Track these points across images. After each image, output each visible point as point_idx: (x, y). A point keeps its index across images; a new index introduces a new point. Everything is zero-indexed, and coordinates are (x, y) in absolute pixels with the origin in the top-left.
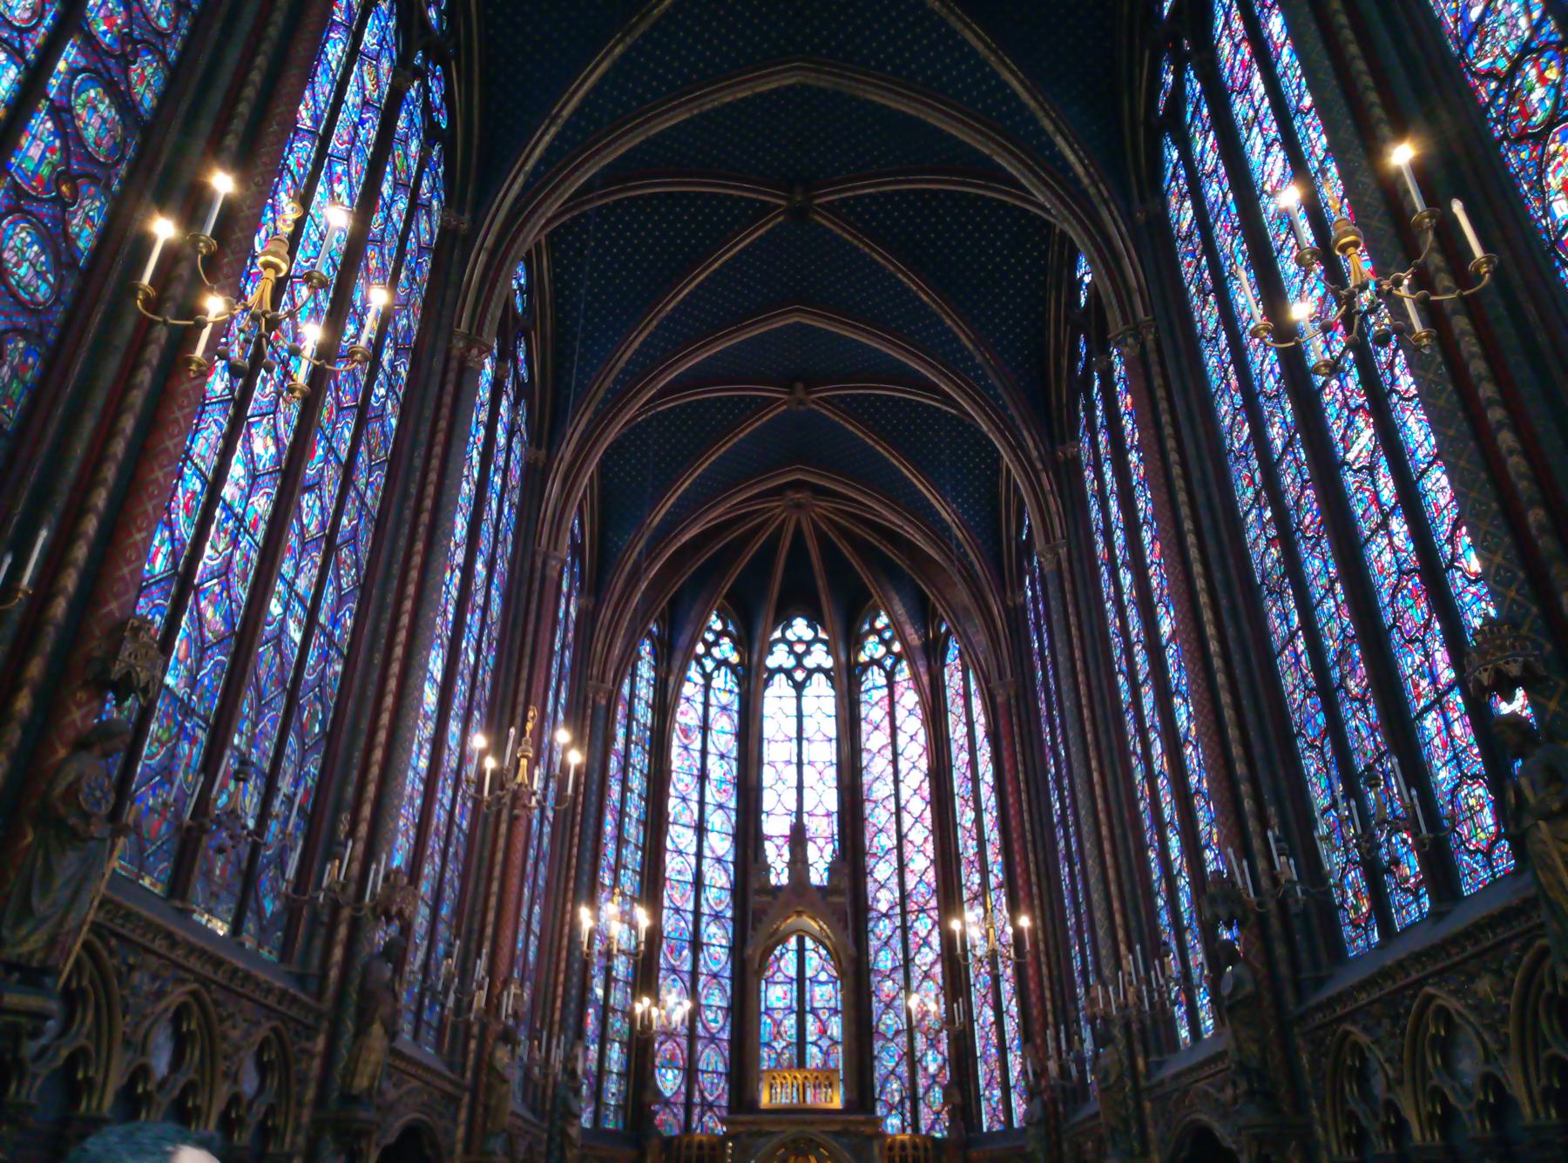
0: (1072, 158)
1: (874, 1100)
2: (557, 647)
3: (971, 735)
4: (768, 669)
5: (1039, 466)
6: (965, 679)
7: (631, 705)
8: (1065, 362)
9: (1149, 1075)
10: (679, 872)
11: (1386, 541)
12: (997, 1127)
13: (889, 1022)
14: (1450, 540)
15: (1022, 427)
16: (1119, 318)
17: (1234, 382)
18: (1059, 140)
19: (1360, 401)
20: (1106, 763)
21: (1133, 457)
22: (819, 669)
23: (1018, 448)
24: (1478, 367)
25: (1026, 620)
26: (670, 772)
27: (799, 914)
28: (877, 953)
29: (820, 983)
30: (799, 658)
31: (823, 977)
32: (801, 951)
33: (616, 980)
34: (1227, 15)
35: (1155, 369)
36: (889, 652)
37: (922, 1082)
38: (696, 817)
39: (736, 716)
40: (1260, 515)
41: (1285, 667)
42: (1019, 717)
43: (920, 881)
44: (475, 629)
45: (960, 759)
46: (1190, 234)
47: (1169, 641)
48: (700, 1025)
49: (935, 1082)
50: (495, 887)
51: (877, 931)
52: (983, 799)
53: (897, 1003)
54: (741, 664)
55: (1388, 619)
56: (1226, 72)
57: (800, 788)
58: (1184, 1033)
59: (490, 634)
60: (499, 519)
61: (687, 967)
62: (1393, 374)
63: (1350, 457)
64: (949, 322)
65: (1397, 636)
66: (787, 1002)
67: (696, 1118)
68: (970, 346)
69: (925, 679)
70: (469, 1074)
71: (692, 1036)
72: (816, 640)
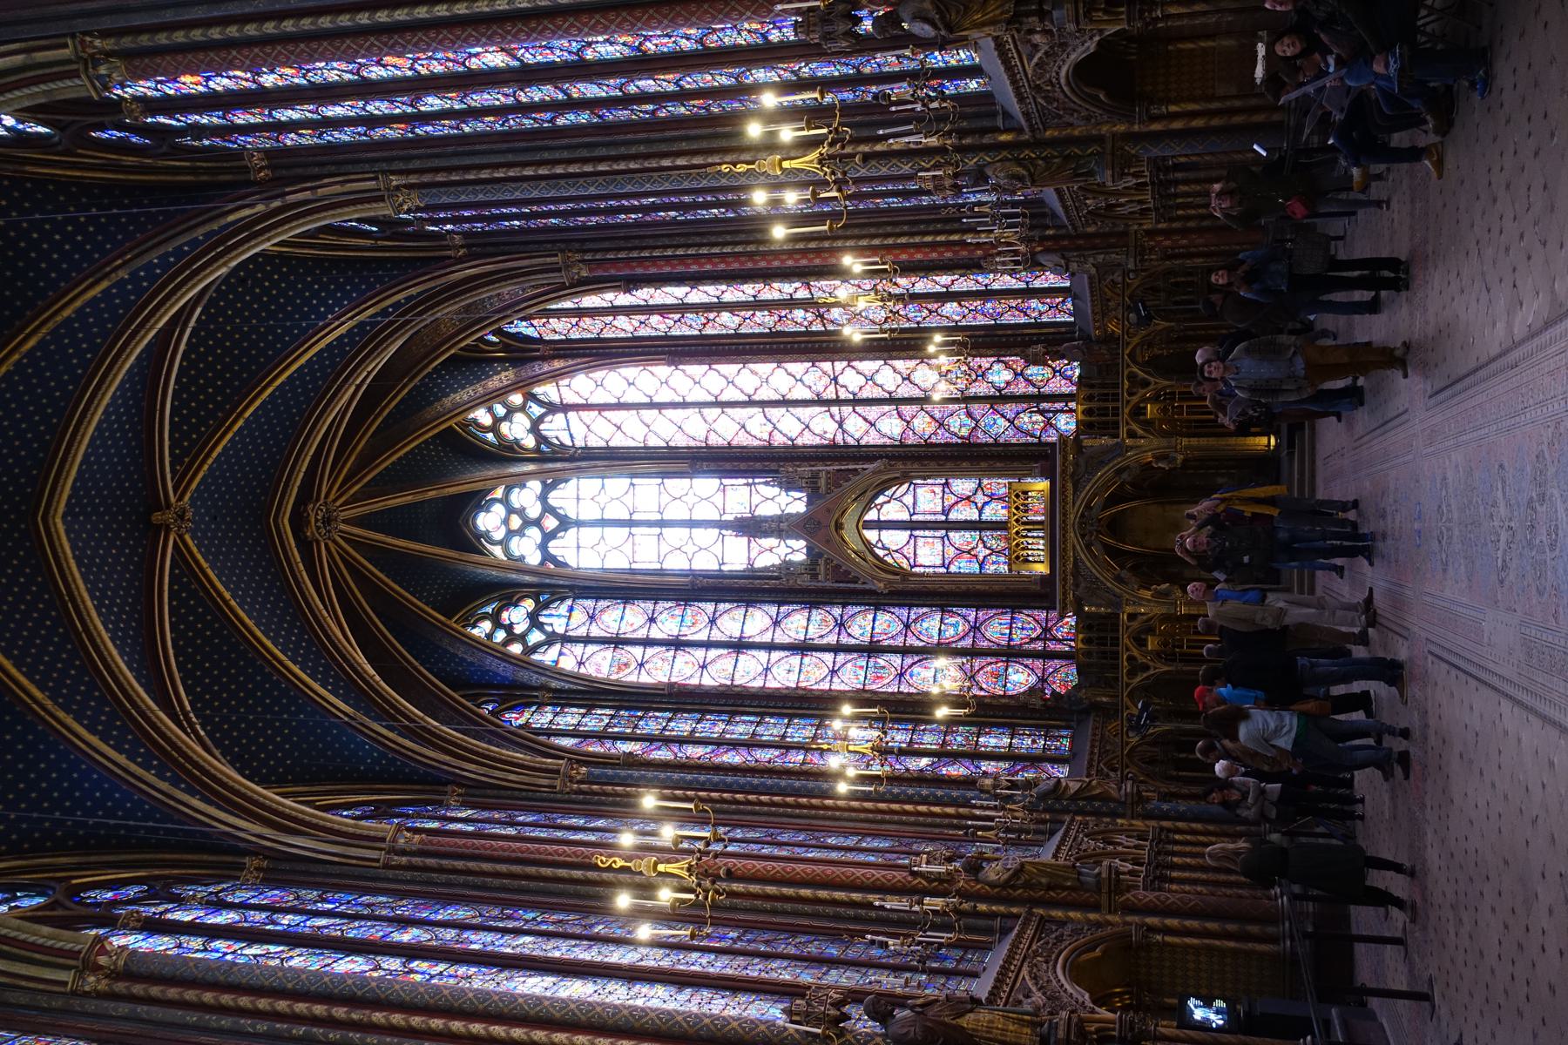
1: (1040, 444)
2: (511, 831)
3: (629, 311)
4: (542, 563)
5: (276, 204)
6: (559, 314)
7: (586, 736)
8: (130, 160)
9: (1020, 130)
12: (1069, 305)
13: (959, 424)
15: (223, 222)
16: (69, 83)
20: (664, 148)
21: (268, 80)
22: (543, 498)
23: (251, 228)
25: (484, 233)
26: (671, 685)
27: (839, 526)
30: (527, 523)
31: (908, 499)
32: (881, 525)
35: (144, 40)
36: (522, 409)
37: (1021, 388)
38: (725, 651)
39: (602, 604)
42: (608, 250)
44: (489, 937)
45: (657, 325)
47: (514, 57)
48: (960, 645)
49: (1022, 374)
50: (806, 892)
52: (705, 299)
53: (938, 416)
57: (692, 524)
58: (973, 85)
59: (495, 918)
60: (342, 915)
61: (896, 660)
64: (66, 313)
67: (1059, 647)
68: (105, 284)
69: (557, 364)
70: (1015, 910)
71: (972, 653)
72: (505, 501)
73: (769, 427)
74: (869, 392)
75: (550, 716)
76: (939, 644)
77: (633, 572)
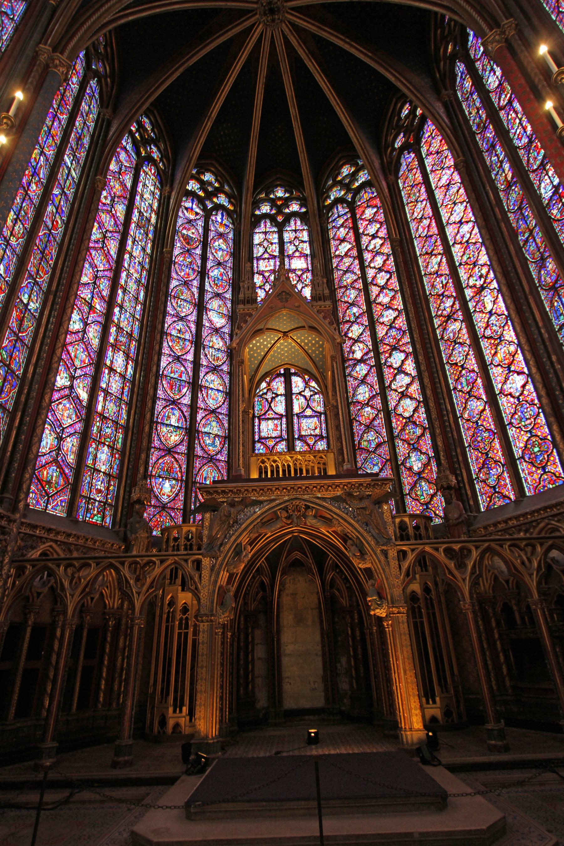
4: (253, 215)
10: (179, 331)
12: (499, 503)
22: (294, 214)
28: (355, 389)
29: (306, 417)
31: (309, 412)
32: (289, 395)
33: (107, 392)
37: (407, 480)
38: (196, 296)
43: (391, 327)
51: (354, 373)
52: (449, 238)
53: (376, 423)
54: (235, 211)
61: (186, 400)
66: (279, 432)
71: (190, 455)
73: (352, 319)
74: (387, 373)
75: (152, 189)
76: (198, 432)
77: (251, 258)
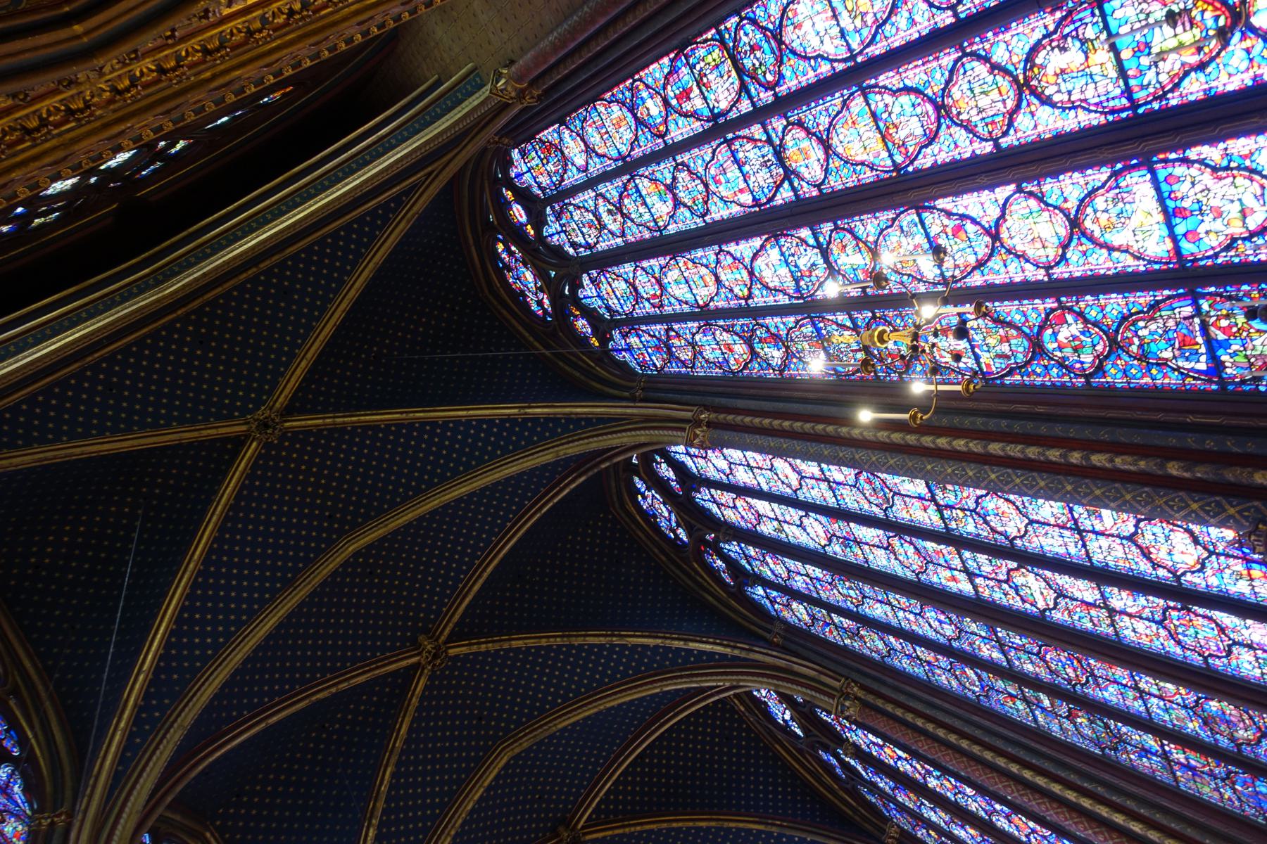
0: (708, 647)
8: (828, 780)
11: (1126, 618)
14: (1155, 565)
17: (929, 656)
18: (692, 645)
19: (1004, 569)
21: (932, 783)
24: (1032, 452)
34: (715, 502)
35: (880, 703)
40: (1044, 709)
41: (1191, 784)
46: (813, 617)
55: (1197, 660)
56: (743, 524)
62: (1001, 533)
63: (1041, 604)
64: (732, 825)
65: (1217, 662)
68: (761, 827)
